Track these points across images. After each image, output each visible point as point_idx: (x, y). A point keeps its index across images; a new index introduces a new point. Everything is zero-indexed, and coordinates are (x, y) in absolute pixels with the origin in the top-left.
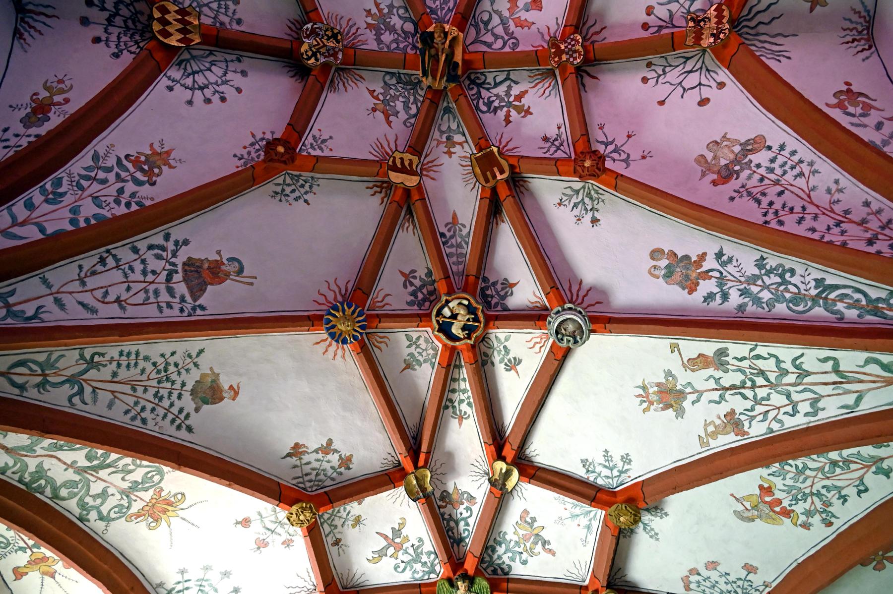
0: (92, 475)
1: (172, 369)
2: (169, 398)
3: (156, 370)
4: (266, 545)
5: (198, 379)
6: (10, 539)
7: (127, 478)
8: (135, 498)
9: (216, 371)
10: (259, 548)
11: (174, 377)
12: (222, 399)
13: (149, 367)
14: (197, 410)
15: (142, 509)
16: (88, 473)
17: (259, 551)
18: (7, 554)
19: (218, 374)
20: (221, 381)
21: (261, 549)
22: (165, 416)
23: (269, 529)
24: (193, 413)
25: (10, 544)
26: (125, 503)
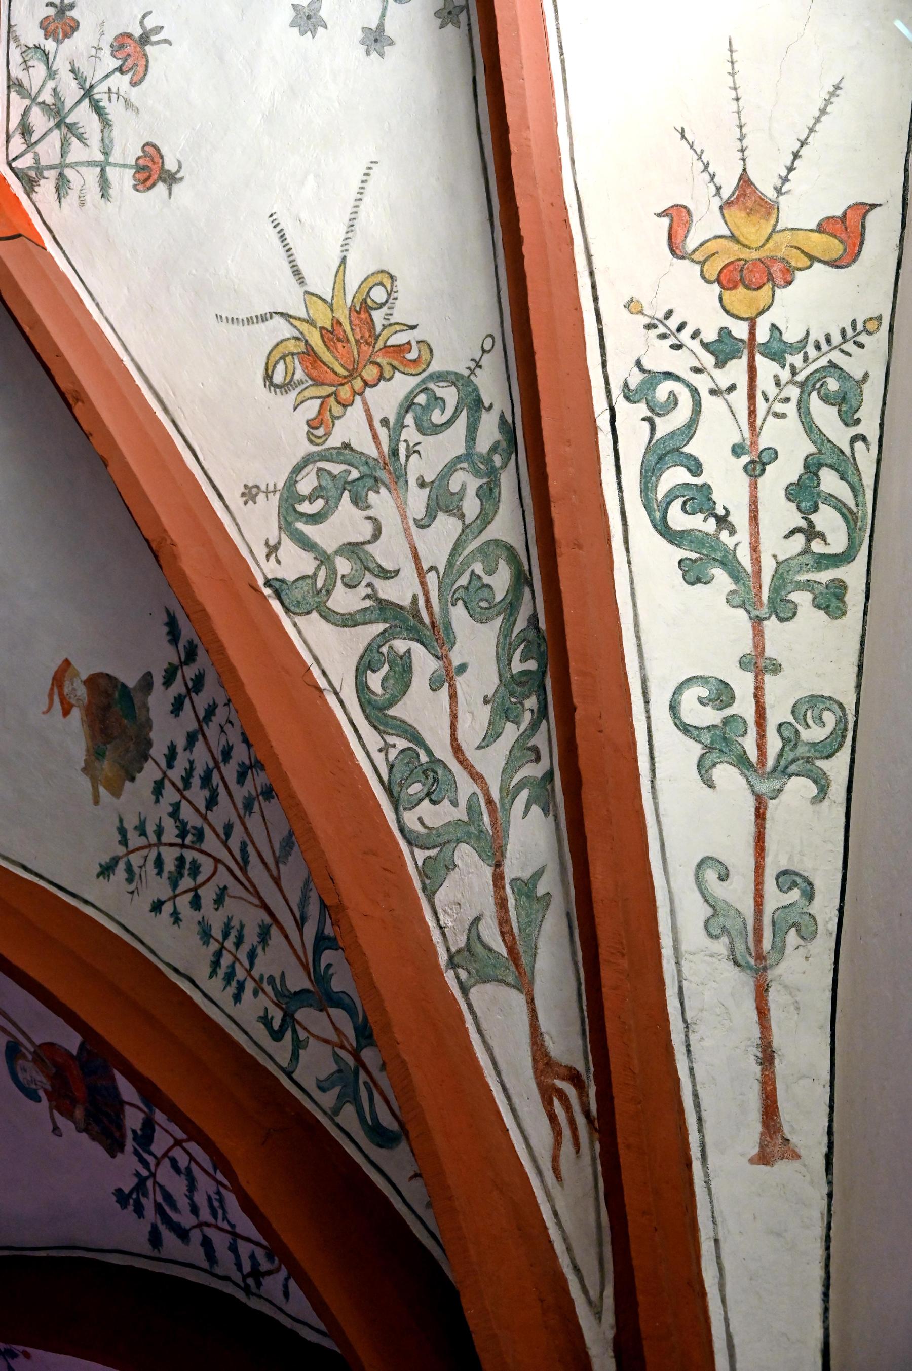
0: (428, 601)
1: (170, 865)
2: (191, 763)
3: (200, 879)
4: (121, 42)
5: (128, 784)
6: (791, 409)
7: (367, 530)
8: (383, 433)
9: (85, 783)
10: (145, 39)
11: (169, 824)
12: (92, 682)
13: (208, 894)
14: (147, 682)
15: (381, 377)
16: (431, 613)
17: (150, 23)
18: (836, 339)
19: (84, 770)
20: (83, 745)
21: (137, 32)
22: (211, 711)
23: (98, 109)
24: (158, 680)
25: (802, 385)
26: (410, 434)
